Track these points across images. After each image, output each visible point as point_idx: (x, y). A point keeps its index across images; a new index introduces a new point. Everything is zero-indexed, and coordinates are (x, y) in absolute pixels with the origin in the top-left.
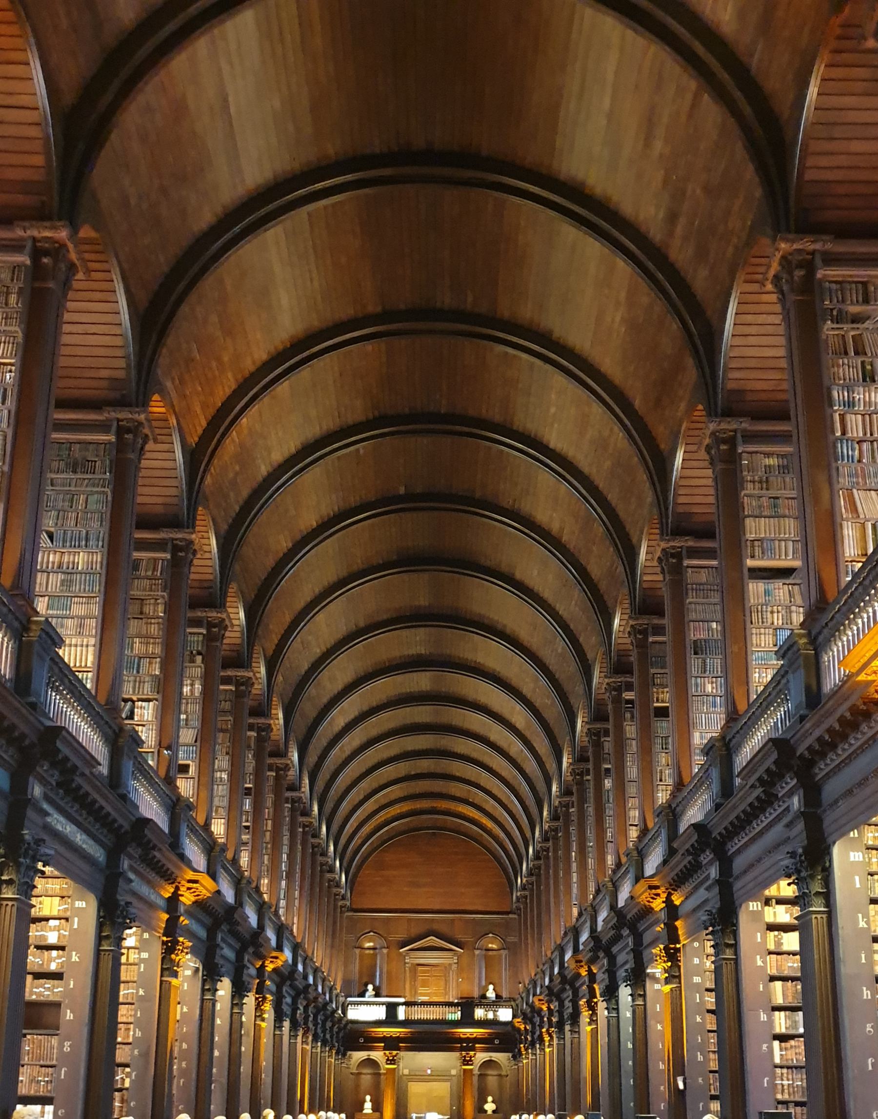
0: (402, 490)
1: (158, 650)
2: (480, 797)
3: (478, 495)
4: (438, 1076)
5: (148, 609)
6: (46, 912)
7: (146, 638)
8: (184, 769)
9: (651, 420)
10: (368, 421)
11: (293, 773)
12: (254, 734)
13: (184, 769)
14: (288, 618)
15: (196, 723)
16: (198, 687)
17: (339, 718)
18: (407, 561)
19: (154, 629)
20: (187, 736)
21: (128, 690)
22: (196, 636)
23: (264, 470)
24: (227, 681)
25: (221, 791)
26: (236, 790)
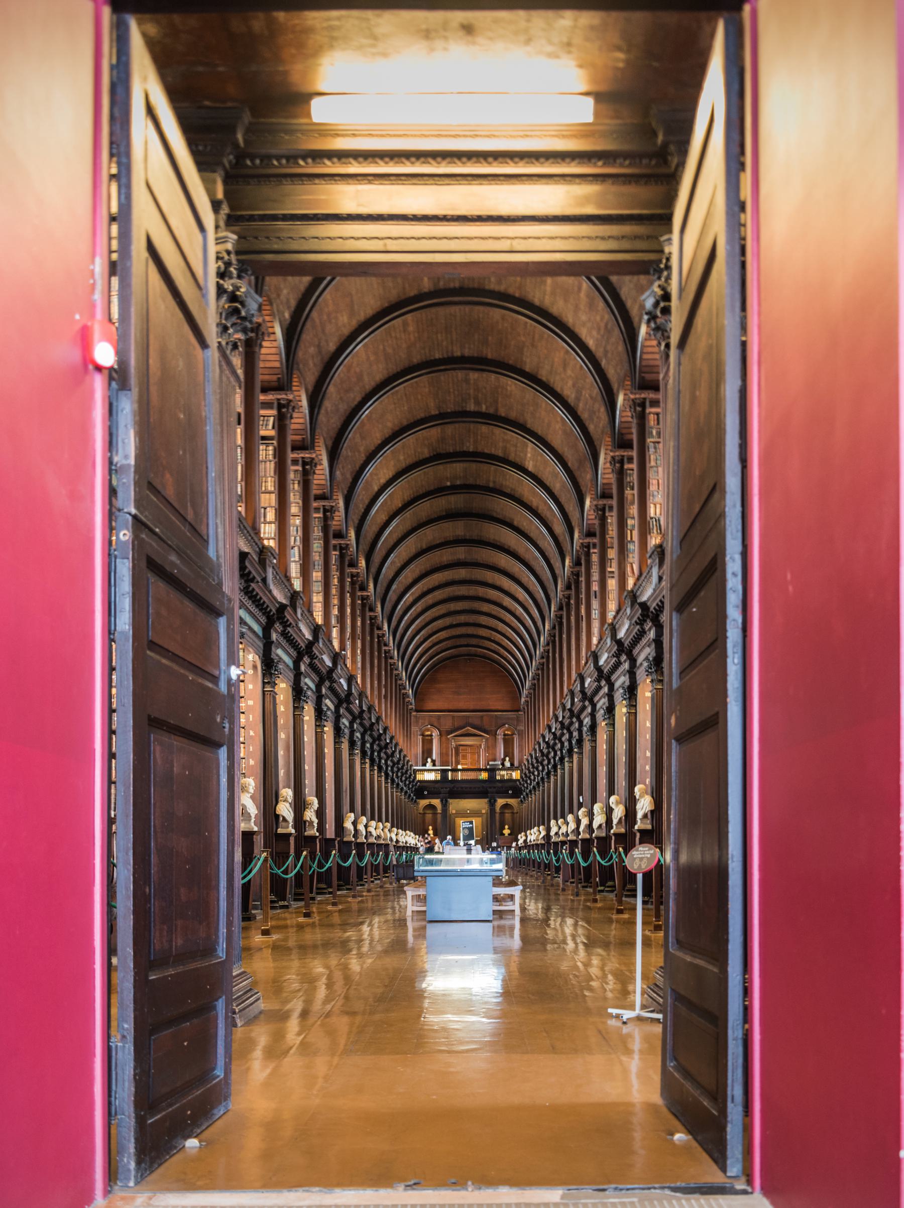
0: (449, 484)
2: (498, 637)
3: (491, 485)
9: (577, 474)
10: (431, 457)
23: (376, 488)
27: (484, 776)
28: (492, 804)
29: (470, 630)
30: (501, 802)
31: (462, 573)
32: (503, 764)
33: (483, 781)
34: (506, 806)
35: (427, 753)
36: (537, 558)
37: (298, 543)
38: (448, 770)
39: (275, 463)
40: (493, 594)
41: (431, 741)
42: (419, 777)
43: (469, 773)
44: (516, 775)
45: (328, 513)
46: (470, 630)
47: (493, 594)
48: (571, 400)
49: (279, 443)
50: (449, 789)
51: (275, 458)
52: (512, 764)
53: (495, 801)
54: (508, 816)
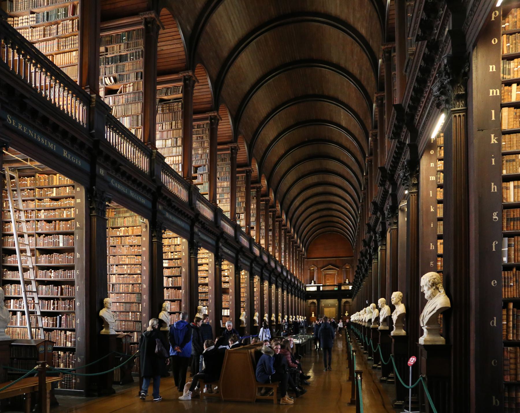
1: (244, 200)
4: (332, 306)
5: (242, 189)
6: (224, 269)
7: (242, 197)
8: (253, 228)
11: (284, 222)
12: (271, 213)
13: (253, 228)
14: (279, 178)
15: (255, 216)
16: (255, 205)
17: (297, 203)
18: (310, 157)
19: (243, 195)
20: (253, 219)
21: (238, 211)
22: (253, 192)
24: (263, 201)
25: (263, 232)
26: (267, 230)
27: (336, 289)
28: (340, 301)
29: (329, 219)
30: (344, 300)
31: (320, 189)
32: (345, 283)
33: (336, 290)
34: (346, 302)
35: (312, 278)
36: (352, 177)
37: (207, 163)
38: (320, 286)
39: (182, 112)
40: (337, 199)
41: (314, 273)
42: (308, 289)
43: (330, 287)
44: (350, 287)
45: (234, 151)
46: (329, 219)
47: (337, 199)
48: (358, 76)
49: (184, 102)
50: (319, 295)
51: (182, 109)
52: (349, 282)
53: (341, 300)
54: (347, 307)
